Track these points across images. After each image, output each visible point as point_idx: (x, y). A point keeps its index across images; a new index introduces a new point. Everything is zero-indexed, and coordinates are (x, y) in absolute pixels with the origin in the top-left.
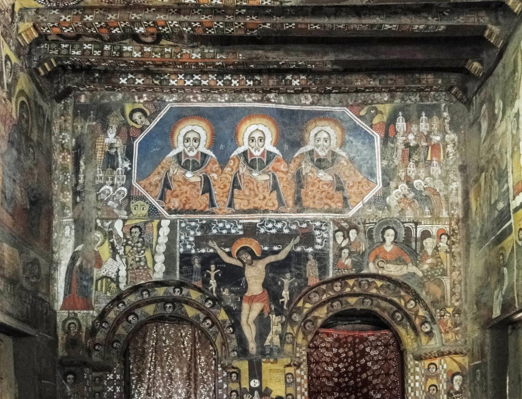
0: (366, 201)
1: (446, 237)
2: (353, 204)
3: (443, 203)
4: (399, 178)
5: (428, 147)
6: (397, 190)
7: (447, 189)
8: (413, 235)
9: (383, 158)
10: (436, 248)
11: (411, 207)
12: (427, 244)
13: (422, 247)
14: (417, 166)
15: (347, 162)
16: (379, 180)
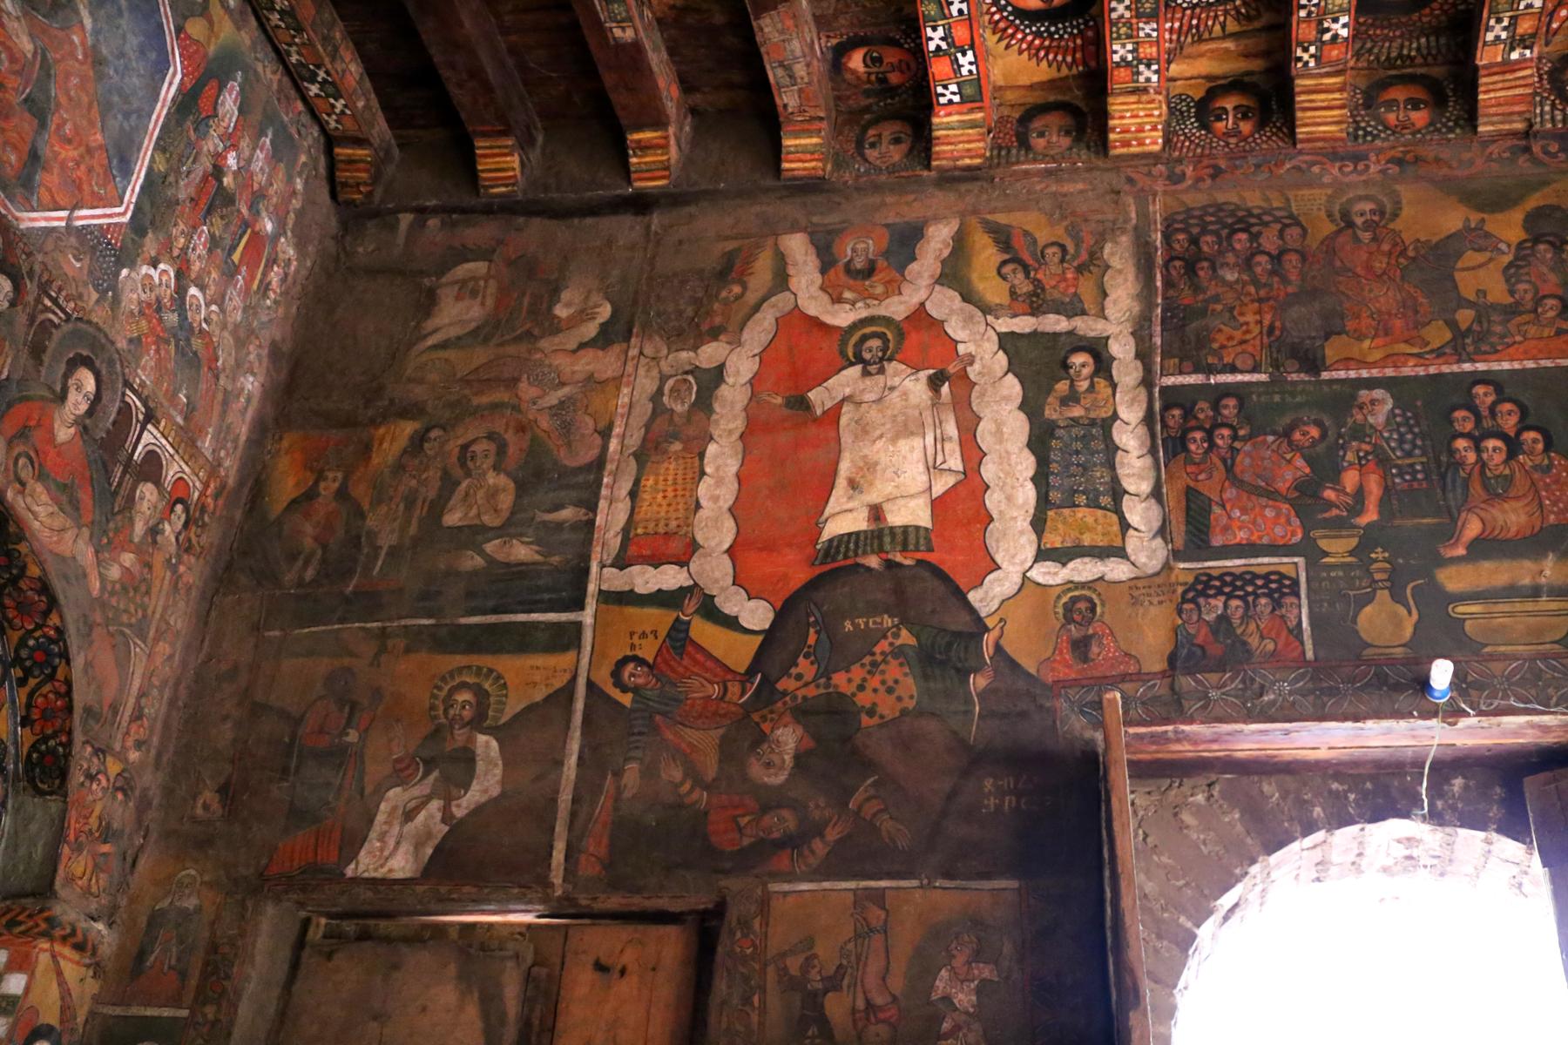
0: (79, 223)
1: (183, 517)
2: (46, 197)
3: (217, 408)
4: (168, 245)
5: (246, 225)
6: (152, 271)
7: (234, 380)
8: (128, 446)
9: (161, 147)
10: (154, 531)
11: (157, 351)
12: (142, 499)
13: (131, 500)
14: (210, 251)
15: (85, 55)
16: (132, 195)
